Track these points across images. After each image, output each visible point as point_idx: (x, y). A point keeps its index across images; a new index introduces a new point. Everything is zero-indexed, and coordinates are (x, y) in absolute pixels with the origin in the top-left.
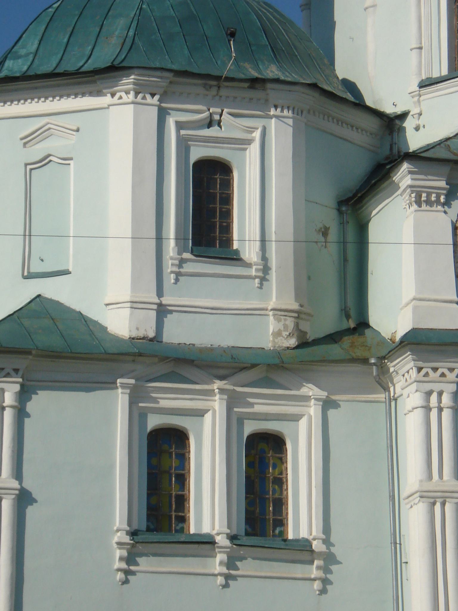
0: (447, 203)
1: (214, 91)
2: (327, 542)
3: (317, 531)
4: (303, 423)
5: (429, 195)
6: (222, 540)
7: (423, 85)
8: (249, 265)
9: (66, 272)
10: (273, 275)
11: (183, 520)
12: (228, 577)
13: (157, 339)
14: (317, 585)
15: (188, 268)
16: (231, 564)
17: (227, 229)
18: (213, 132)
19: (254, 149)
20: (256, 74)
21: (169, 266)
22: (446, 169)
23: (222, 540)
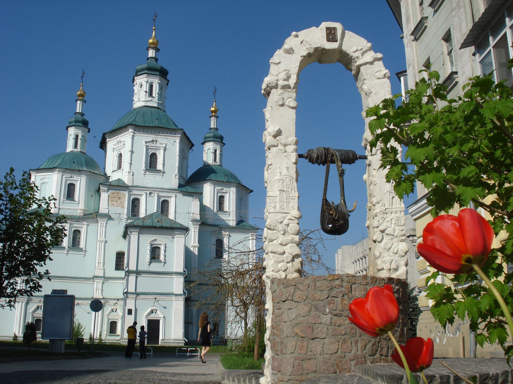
0: (108, 192)
2: (85, 248)
3: (84, 247)
4: (83, 228)
6: (67, 248)
10: (80, 203)
12: (67, 254)
13: (58, 213)
14: (83, 255)
15: (65, 202)
16: (68, 251)
17: (74, 195)
18: (72, 179)
19: (79, 181)
20: (81, 169)
21: (61, 201)
22: (107, 186)
23: (67, 248)
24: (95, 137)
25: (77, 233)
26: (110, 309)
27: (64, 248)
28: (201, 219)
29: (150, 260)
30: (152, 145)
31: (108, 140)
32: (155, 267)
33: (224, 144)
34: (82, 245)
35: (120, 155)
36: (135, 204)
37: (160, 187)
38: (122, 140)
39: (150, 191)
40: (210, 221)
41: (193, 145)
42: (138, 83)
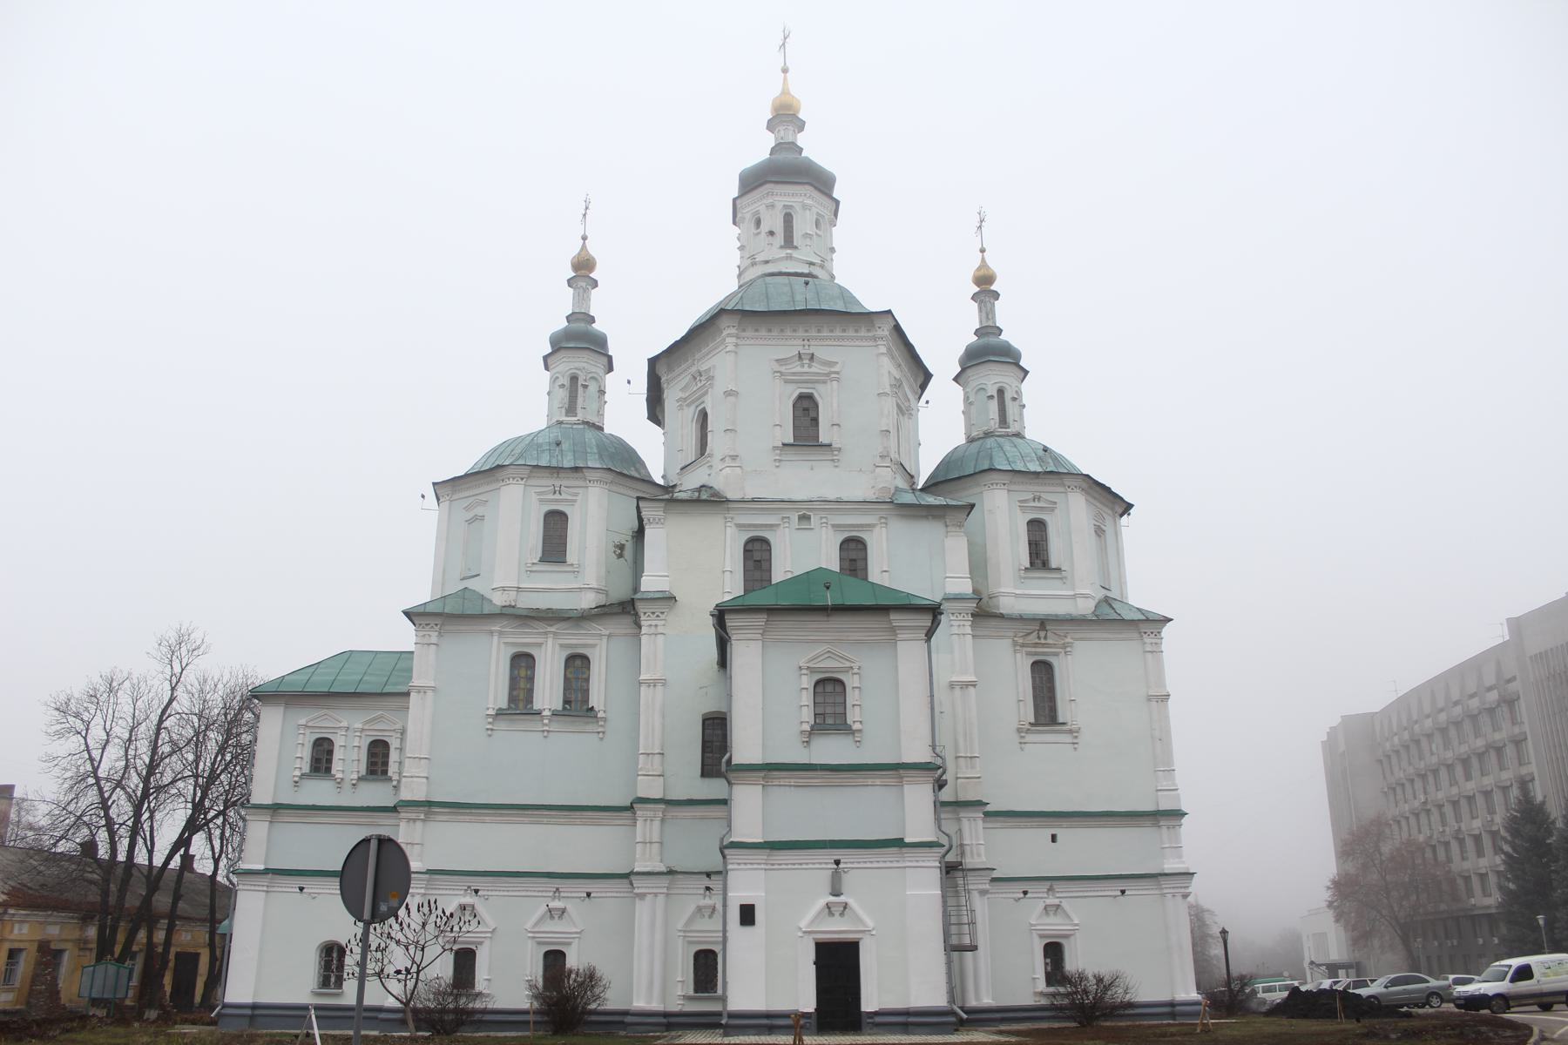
1: (555, 475)
5: (654, 519)
7: (682, 469)
8: (572, 565)
9: (479, 575)
11: (532, 702)
18: (557, 496)
24: (629, 382)
25: (577, 664)
26: (692, 908)
27: (539, 713)
28: (974, 591)
29: (812, 728)
30: (799, 369)
31: (663, 379)
32: (831, 750)
33: (1026, 372)
34: (595, 700)
35: (704, 416)
36: (757, 554)
37: (832, 495)
38: (703, 367)
39: (805, 512)
40: (1007, 605)
41: (927, 376)
42: (748, 216)
